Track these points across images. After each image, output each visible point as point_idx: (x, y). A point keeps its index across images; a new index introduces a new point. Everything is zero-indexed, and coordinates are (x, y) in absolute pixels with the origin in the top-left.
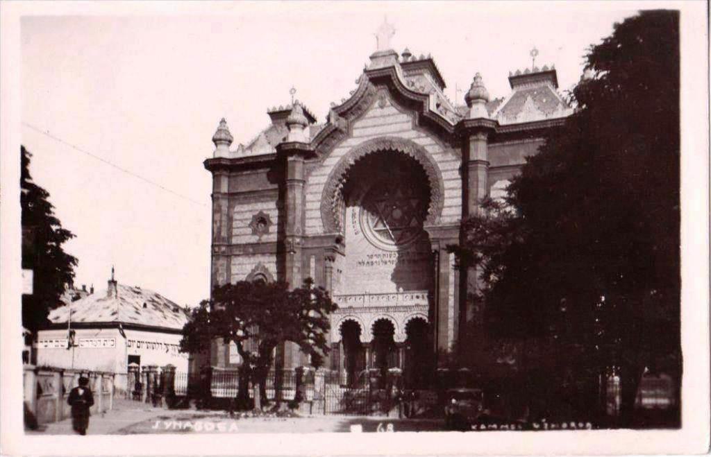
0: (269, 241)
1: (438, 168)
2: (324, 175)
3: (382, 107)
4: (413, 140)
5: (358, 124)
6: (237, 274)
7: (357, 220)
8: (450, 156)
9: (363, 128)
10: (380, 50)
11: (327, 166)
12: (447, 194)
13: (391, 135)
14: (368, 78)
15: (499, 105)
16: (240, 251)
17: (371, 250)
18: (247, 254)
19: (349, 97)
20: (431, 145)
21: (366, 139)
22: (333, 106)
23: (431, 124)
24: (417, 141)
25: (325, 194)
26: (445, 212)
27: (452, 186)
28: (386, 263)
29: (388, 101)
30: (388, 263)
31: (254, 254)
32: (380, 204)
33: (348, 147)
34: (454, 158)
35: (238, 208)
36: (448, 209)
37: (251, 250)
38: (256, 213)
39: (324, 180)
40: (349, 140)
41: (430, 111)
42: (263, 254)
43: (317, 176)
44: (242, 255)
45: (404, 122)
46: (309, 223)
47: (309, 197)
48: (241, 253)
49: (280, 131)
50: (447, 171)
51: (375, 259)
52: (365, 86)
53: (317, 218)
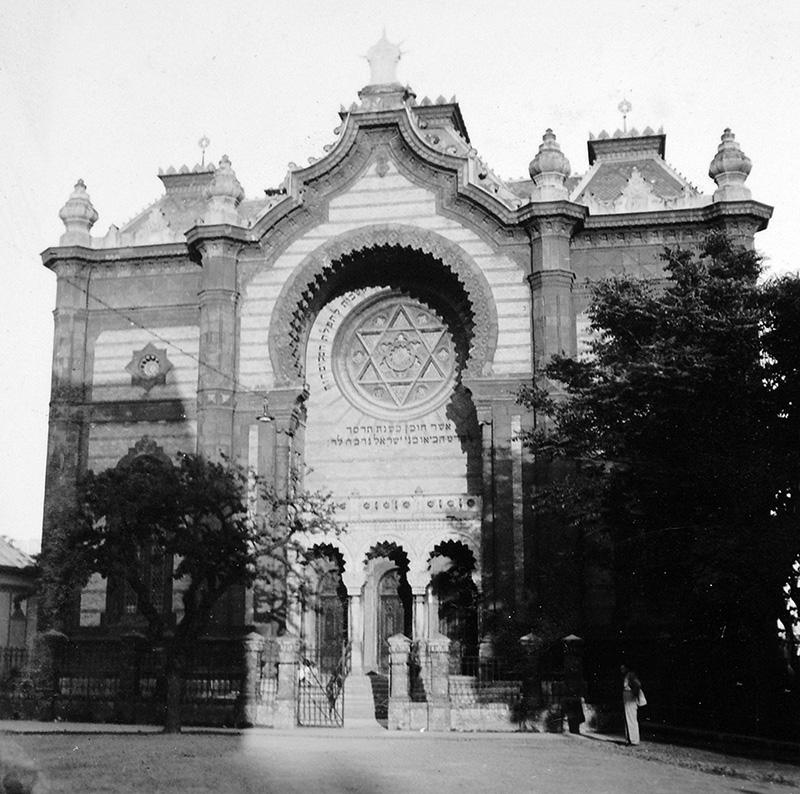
1: (485, 280)
2: (276, 284)
4: (438, 232)
5: (337, 201)
6: (100, 457)
7: (328, 364)
8: (506, 262)
9: (347, 207)
10: (378, 82)
11: (282, 269)
12: (502, 324)
13: (398, 221)
14: (357, 127)
15: (577, 184)
16: (107, 415)
17: (353, 418)
18: (120, 420)
19: (321, 155)
20: (471, 241)
21: (352, 227)
23: (474, 205)
24: (444, 234)
25: (276, 318)
26: (499, 355)
27: (511, 312)
28: (382, 441)
29: (391, 164)
30: (387, 442)
31: (134, 421)
32: (194, 348)
33: (320, 238)
34: (514, 264)
35: (105, 337)
36: (505, 350)
37: (129, 414)
38: (140, 348)
39: (275, 292)
41: (469, 184)
42: (154, 421)
43: (261, 285)
44: (110, 421)
45: (421, 202)
46: (245, 367)
47: (245, 322)
48: (110, 418)
49: (182, 207)
50: (502, 285)
52: (353, 139)
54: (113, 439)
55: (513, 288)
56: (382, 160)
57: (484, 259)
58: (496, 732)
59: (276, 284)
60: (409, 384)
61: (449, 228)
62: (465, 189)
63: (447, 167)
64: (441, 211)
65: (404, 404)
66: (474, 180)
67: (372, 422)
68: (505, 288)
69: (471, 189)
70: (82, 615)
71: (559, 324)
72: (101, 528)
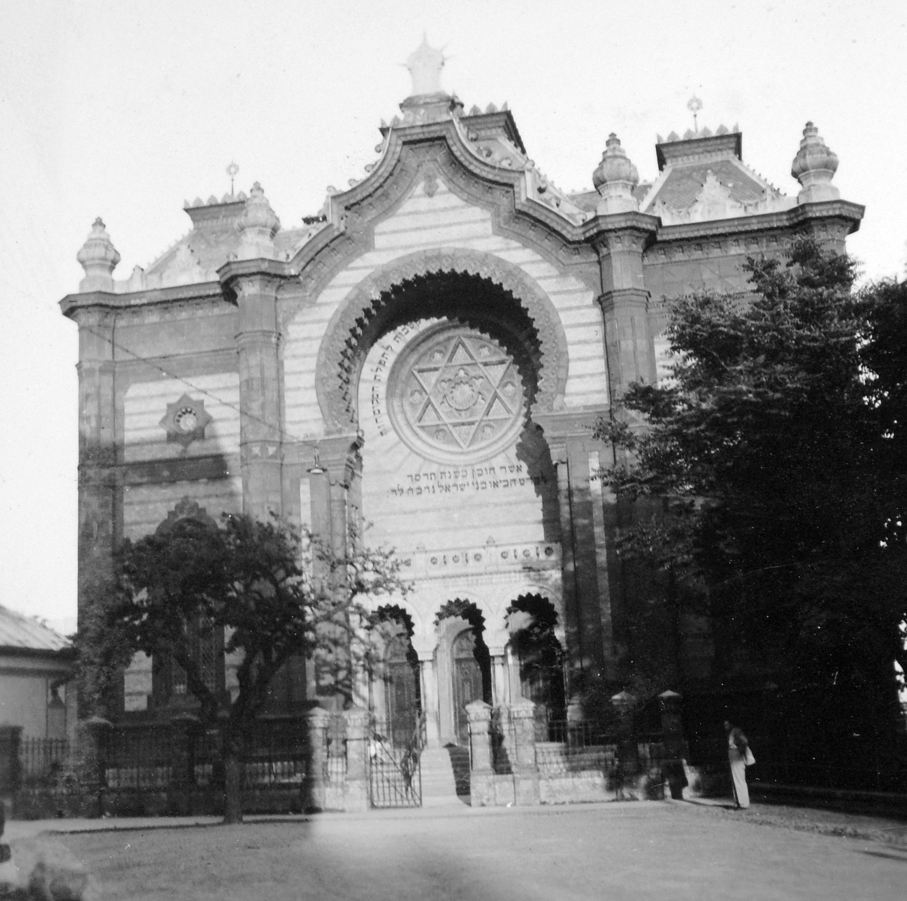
0: (204, 453)
1: (551, 305)
2: (320, 321)
3: (430, 195)
4: (497, 254)
5: (383, 226)
6: (137, 523)
7: (382, 406)
8: (573, 283)
9: (394, 232)
10: (421, 92)
11: (326, 304)
12: (573, 352)
13: (451, 245)
14: (400, 142)
15: (647, 193)
16: (142, 476)
17: (414, 465)
18: (156, 481)
19: (361, 175)
21: (401, 253)
22: (333, 193)
24: (503, 255)
25: (323, 359)
26: (572, 386)
27: (582, 337)
28: (447, 489)
29: (441, 184)
30: (453, 489)
31: (172, 482)
32: (234, 397)
33: (366, 268)
34: (582, 285)
35: (135, 390)
36: (578, 380)
37: (166, 473)
38: (174, 399)
39: (320, 330)
40: (367, 256)
41: (528, 199)
42: (194, 480)
43: (304, 323)
44: (147, 483)
45: (475, 222)
46: (291, 415)
48: (145, 480)
49: (212, 242)
50: (570, 309)
51: (424, 482)
52: (396, 156)
53: (308, 405)
54: (150, 502)
55: (582, 311)
56: (430, 178)
57: (549, 281)
58: (590, 802)
59: (320, 321)
60: (472, 423)
61: (508, 249)
62: (523, 205)
63: (502, 181)
64: (499, 230)
65: (469, 446)
66: (532, 194)
67: (434, 468)
68: (573, 312)
69: (530, 204)
70: (127, 699)
71: (635, 348)
72: (142, 602)
